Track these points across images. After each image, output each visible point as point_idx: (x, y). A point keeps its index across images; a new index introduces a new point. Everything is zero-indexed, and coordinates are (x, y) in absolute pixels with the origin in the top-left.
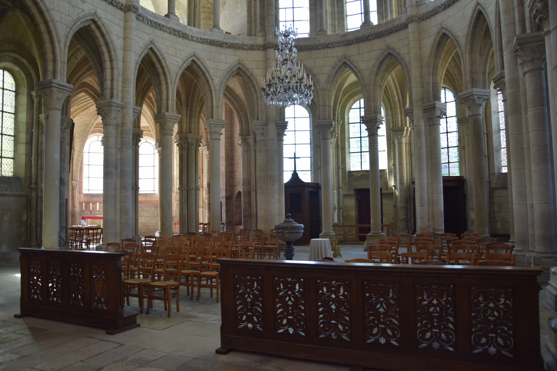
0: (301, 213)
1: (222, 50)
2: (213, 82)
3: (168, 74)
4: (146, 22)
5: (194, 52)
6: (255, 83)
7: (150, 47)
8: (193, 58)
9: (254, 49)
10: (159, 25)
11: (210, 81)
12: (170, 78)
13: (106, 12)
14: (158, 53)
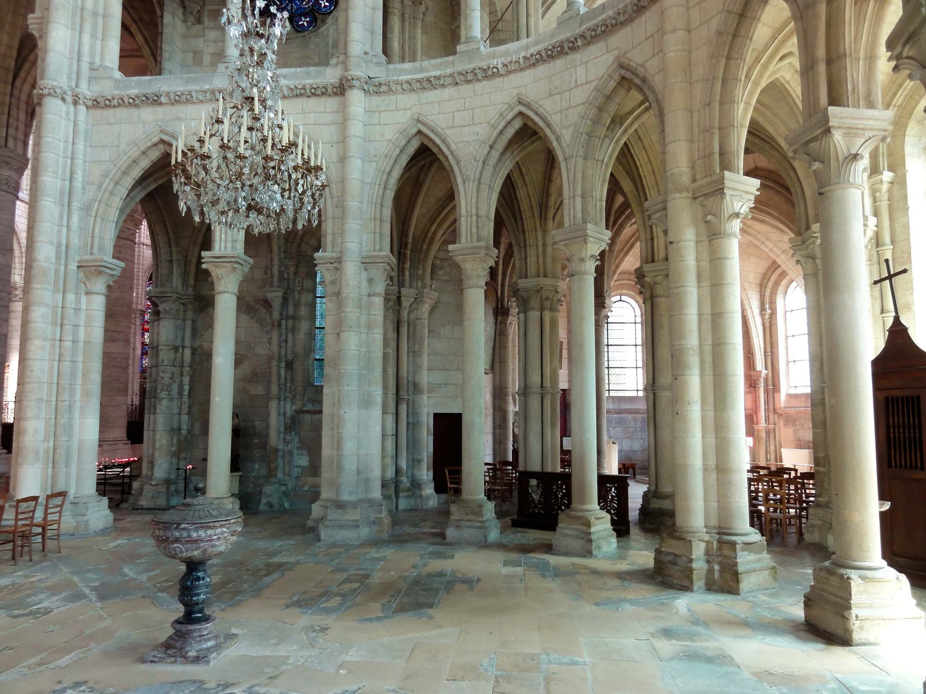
1: (577, 57)
4: (399, 88)
5: (518, 94)
10: (429, 80)
13: (304, 113)
14: (432, 136)
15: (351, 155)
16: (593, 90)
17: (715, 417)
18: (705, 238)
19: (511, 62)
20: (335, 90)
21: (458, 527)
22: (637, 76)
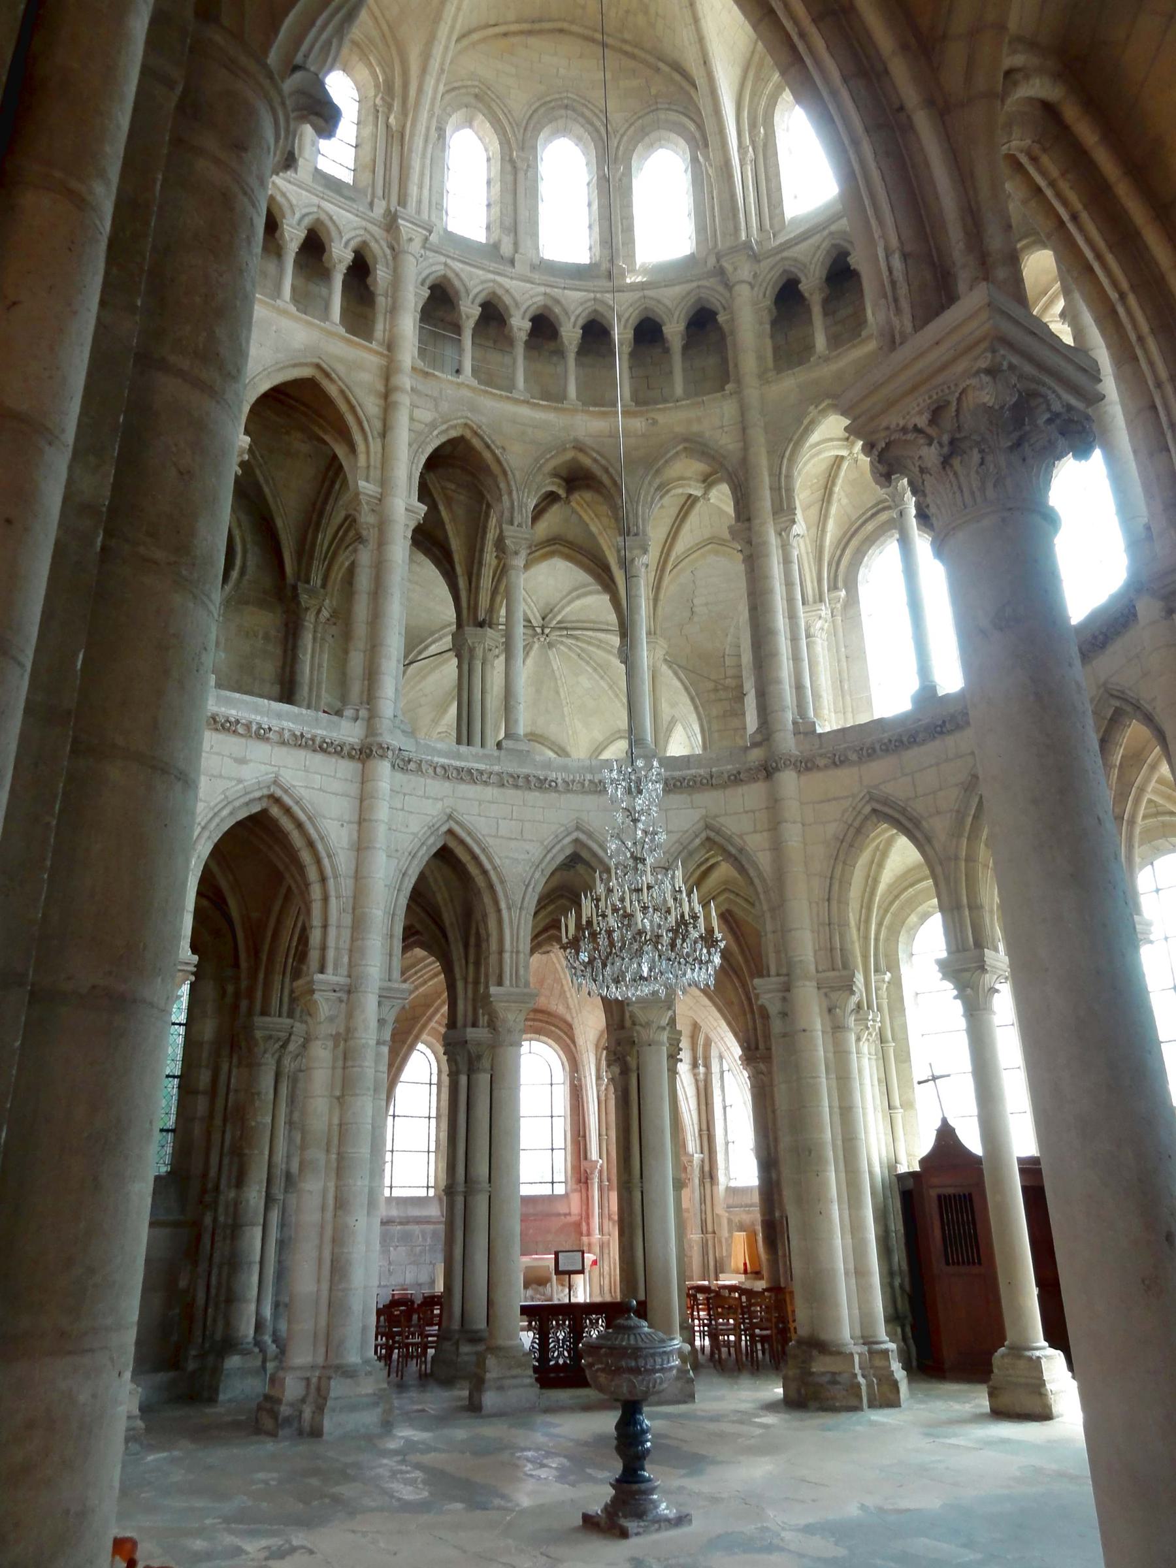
0: (980, 1263)
3: (498, 888)
4: (431, 771)
5: (577, 818)
6: (752, 873)
7: (444, 828)
8: (575, 835)
9: (741, 780)
10: (469, 771)
12: (506, 896)
13: (305, 771)
14: (468, 840)
16: (675, 843)
17: (850, 1216)
18: (829, 1029)
19: (573, 781)
21: (500, 1388)
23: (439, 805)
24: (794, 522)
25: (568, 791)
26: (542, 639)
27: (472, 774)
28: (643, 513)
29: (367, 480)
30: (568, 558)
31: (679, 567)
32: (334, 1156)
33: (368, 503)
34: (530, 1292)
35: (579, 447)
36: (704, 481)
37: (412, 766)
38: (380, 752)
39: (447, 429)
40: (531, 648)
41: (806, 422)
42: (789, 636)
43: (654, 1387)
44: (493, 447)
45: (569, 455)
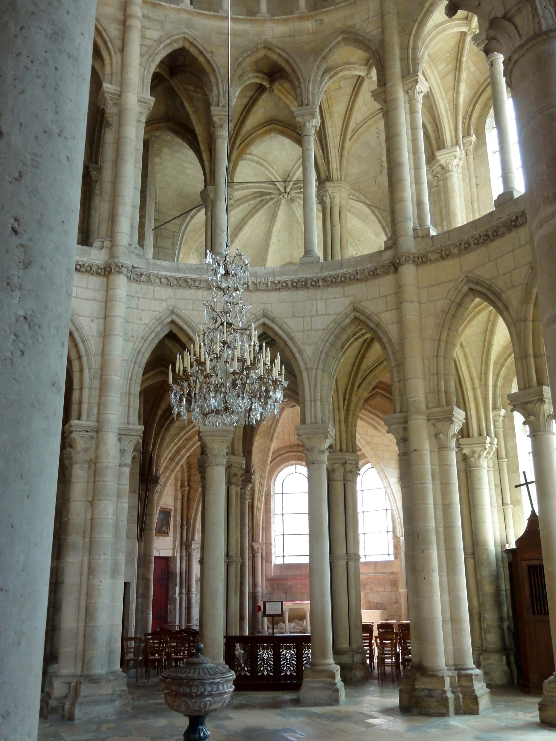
1: (318, 293)
2: (302, 355)
4: (158, 281)
5: (264, 309)
7: (169, 320)
9: (378, 275)
10: (185, 280)
11: (297, 355)
14: (185, 327)
15: (116, 333)
16: (332, 322)
17: (448, 580)
18: (436, 449)
19: (260, 283)
20: (100, 271)
22: (372, 321)
23: (164, 304)
24: (417, 82)
25: (257, 290)
26: (286, 196)
27: (187, 282)
28: (313, 89)
29: (111, 84)
30: (283, 133)
31: (358, 132)
32: (87, 540)
33: (111, 99)
34: (293, 625)
35: (268, 47)
36: (367, 64)
37: (143, 278)
38: (117, 269)
39: (171, 43)
40: (280, 203)
41: (427, 5)
42: (412, 167)
43: (205, 707)
44: (204, 52)
45: (262, 53)
